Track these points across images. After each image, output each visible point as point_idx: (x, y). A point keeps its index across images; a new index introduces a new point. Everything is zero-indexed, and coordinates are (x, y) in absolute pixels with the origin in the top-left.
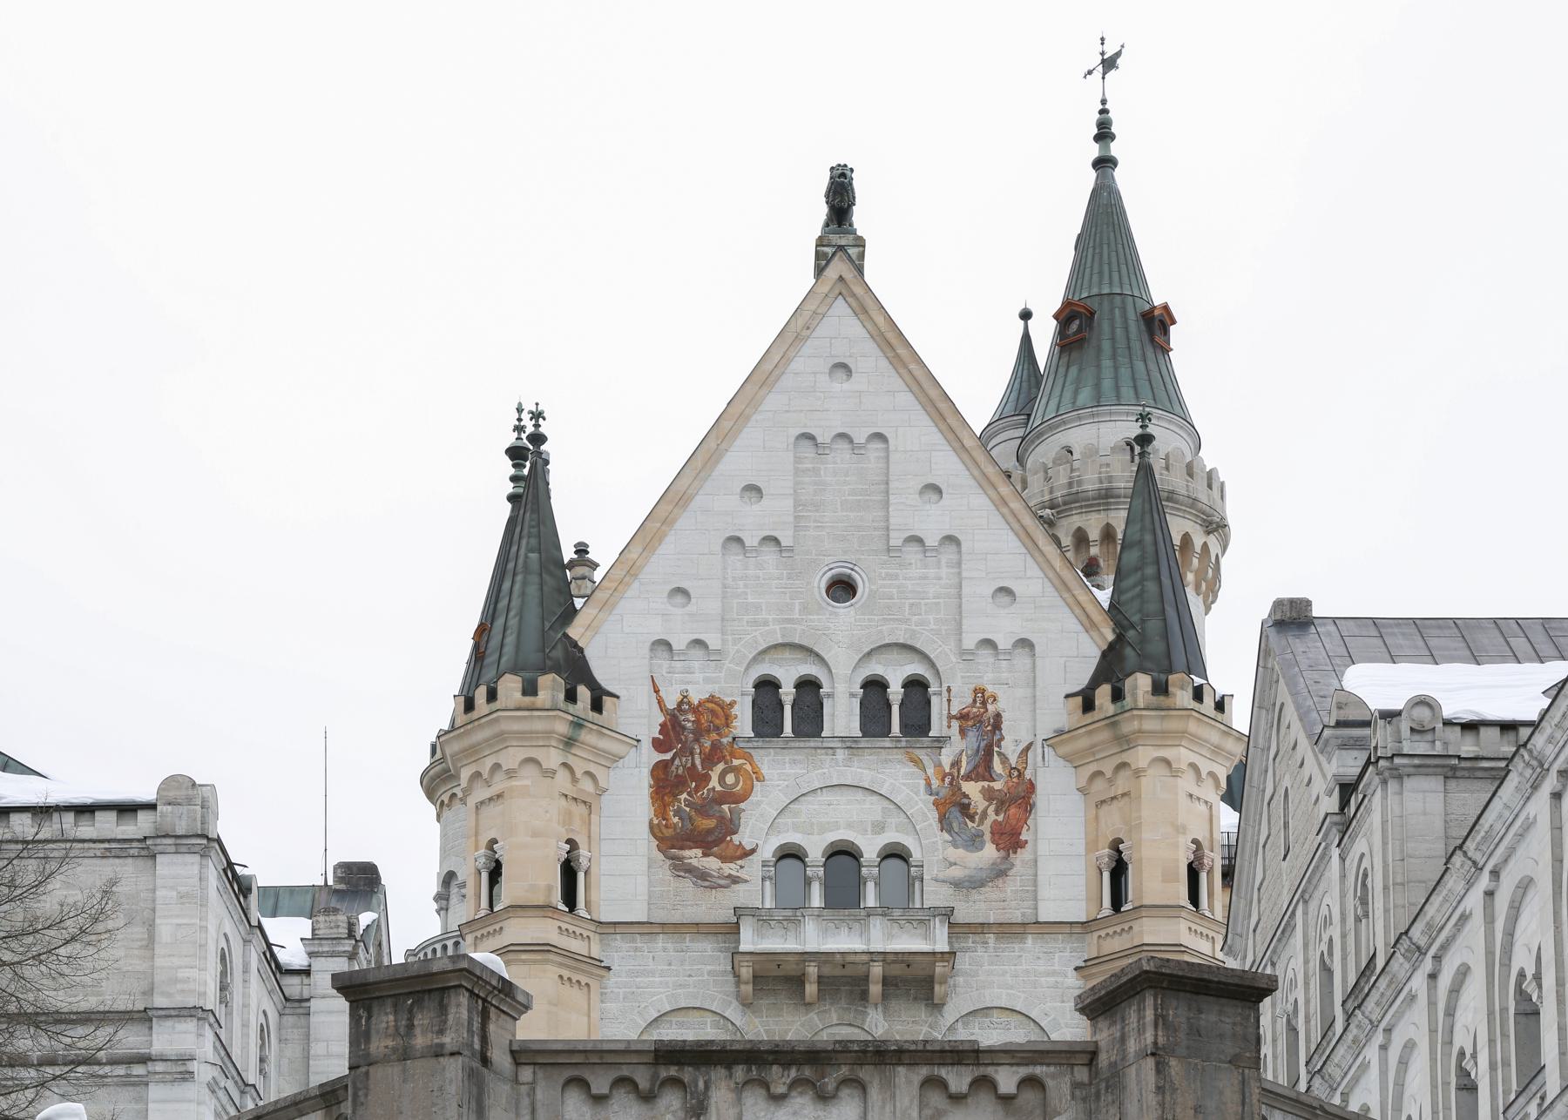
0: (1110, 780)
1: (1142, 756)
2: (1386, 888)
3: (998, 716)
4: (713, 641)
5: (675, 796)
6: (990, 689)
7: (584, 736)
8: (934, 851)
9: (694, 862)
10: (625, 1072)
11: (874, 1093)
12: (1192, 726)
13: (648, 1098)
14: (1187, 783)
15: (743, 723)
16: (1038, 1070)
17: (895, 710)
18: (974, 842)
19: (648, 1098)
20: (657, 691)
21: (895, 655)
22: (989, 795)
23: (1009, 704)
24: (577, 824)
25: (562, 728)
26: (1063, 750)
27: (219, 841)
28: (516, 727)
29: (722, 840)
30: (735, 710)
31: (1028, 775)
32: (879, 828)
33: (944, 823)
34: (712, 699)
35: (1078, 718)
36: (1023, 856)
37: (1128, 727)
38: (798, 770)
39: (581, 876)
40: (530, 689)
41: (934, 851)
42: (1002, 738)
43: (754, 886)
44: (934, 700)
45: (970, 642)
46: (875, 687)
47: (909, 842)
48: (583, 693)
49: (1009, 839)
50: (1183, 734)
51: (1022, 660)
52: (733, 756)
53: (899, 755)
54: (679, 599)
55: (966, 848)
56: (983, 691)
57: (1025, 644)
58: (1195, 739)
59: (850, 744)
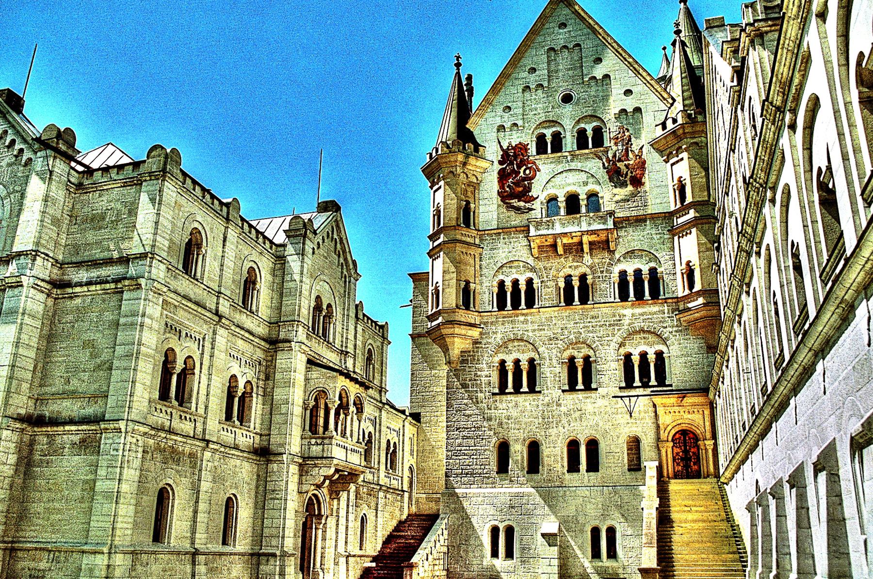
4: (520, 123)
15: (532, 149)
17: (590, 140)
18: (623, 185)
20: (499, 143)
22: (627, 166)
32: (586, 184)
36: (642, 189)
38: (553, 166)
39: (472, 213)
43: (538, 209)
49: (637, 182)
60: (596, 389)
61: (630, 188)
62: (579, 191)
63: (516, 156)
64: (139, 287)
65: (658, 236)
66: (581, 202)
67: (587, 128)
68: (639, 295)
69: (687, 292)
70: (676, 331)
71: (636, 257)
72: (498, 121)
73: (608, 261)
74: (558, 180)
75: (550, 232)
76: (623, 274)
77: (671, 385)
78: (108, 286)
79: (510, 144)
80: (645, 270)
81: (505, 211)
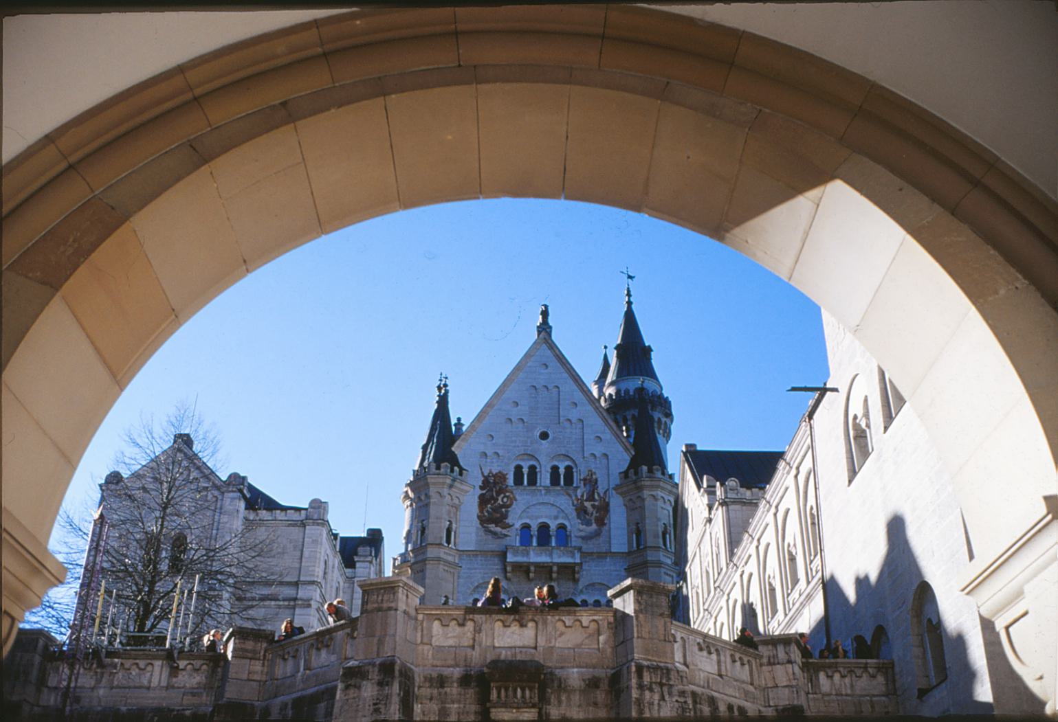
0: (634, 502)
3: (596, 480)
5: (486, 505)
6: (594, 470)
7: (456, 484)
8: (576, 527)
9: (492, 529)
10: (455, 617)
11: (540, 627)
12: (661, 484)
13: (462, 625)
14: (660, 503)
16: (596, 618)
17: (562, 477)
18: (588, 524)
19: (462, 625)
22: (593, 506)
23: (600, 475)
24: (452, 515)
25: (448, 481)
26: (620, 491)
27: (328, 521)
28: (433, 481)
29: (501, 521)
30: (507, 476)
31: (607, 500)
32: (556, 518)
33: (579, 517)
34: (500, 472)
37: (639, 484)
38: (529, 497)
39: (453, 533)
40: (438, 468)
41: (576, 527)
44: (575, 474)
46: (555, 469)
47: (567, 523)
48: (456, 468)
49: (601, 522)
50: (658, 487)
52: (507, 492)
54: (490, 439)
55: (587, 525)
56: (591, 471)
57: (606, 455)
58: (663, 489)
61: (594, 526)
62: (549, 522)
63: (495, 483)
64: (309, 606)
65: (617, 573)
66: (551, 533)
67: (560, 466)
72: (482, 448)
73: (572, 590)
75: (525, 559)
78: (281, 603)
79: (490, 472)
81: (483, 534)
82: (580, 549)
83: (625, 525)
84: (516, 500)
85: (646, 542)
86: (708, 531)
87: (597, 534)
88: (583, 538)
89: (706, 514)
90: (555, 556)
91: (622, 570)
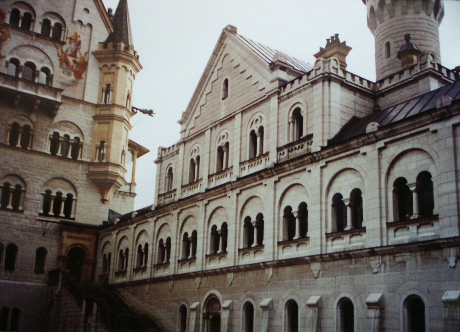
1: (120, 64)
2: (323, 115)
6: (79, 34)
12: (134, 61)
18: (69, 74)
21: (54, 16)
22: (75, 62)
23: (83, 38)
26: (98, 56)
31: (86, 60)
35: (102, 49)
36: (82, 81)
42: (80, 48)
44: (63, 32)
45: (75, 19)
47: (50, 68)
51: (88, 29)
53: (50, 43)
55: (66, 75)
57: (90, 25)
59: (37, 35)
60: (22, 212)
61: (73, 77)
68: (65, 152)
69: (97, 161)
70: (84, 184)
71: (67, 126)
74: (24, 50)
75: (13, 88)
76: (56, 134)
77: (74, 219)
80: (72, 137)
82: (61, 90)
83: (97, 84)
84: (10, 37)
85: (114, 99)
86: (274, 100)
87: (74, 83)
88: (62, 84)
89: (276, 84)
90: (39, 91)
91: (91, 117)
